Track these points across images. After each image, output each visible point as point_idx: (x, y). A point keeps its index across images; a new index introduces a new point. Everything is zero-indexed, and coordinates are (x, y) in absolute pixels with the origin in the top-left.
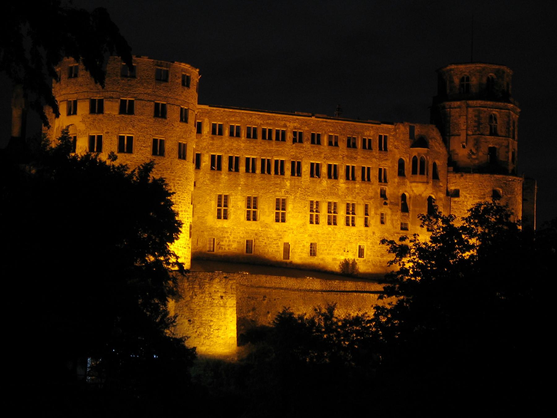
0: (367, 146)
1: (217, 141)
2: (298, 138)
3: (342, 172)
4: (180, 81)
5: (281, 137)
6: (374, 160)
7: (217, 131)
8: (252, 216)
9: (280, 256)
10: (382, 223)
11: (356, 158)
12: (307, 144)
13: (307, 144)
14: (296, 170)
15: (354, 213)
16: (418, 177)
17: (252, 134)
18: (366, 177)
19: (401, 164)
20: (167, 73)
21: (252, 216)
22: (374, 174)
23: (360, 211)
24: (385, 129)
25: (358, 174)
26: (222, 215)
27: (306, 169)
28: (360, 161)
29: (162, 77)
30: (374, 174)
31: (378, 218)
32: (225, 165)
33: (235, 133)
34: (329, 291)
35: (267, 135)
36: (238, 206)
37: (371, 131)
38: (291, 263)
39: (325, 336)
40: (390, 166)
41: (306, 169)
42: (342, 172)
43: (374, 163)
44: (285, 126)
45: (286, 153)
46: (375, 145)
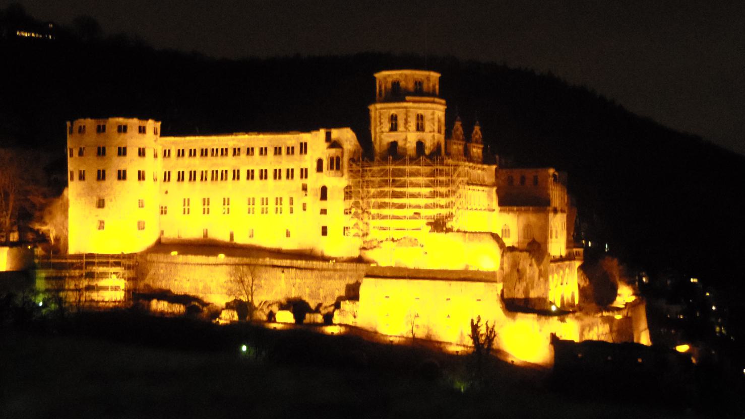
0: (290, 151)
1: (181, 160)
2: (236, 152)
3: (270, 174)
4: (116, 129)
5: (224, 152)
6: (296, 162)
7: (181, 154)
8: (206, 211)
9: (227, 239)
10: (304, 209)
11: (281, 162)
12: (243, 155)
13: (243, 155)
14: (236, 175)
15: (281, 204)
16: (332, 172)
17: (204, 153)
18: (290, 174)
19: (320, 162)
20: (104, 127)
21: (206, 211)
22: (297, 173)
23: (286, 202)
24: (305, 137)
25: (284, 174)
26: (186, 212)
27: (243, 175)
28: (285, 163)
29: (101, 130)
30: (297, 173)
31: (301, 207)
32: (187, 176)
33: (192, 153)
34: (214, 265)
35: (215, 152)
36: (196, 206)
37: (291, 139)
38: (235, 243)
39: (720, 320)
40: (312, 166)
41: (243, 175)
42: (270, 174)
43: (295, 163)
44: (227, 145)
45: (228, 163)
46: (297, 150)
